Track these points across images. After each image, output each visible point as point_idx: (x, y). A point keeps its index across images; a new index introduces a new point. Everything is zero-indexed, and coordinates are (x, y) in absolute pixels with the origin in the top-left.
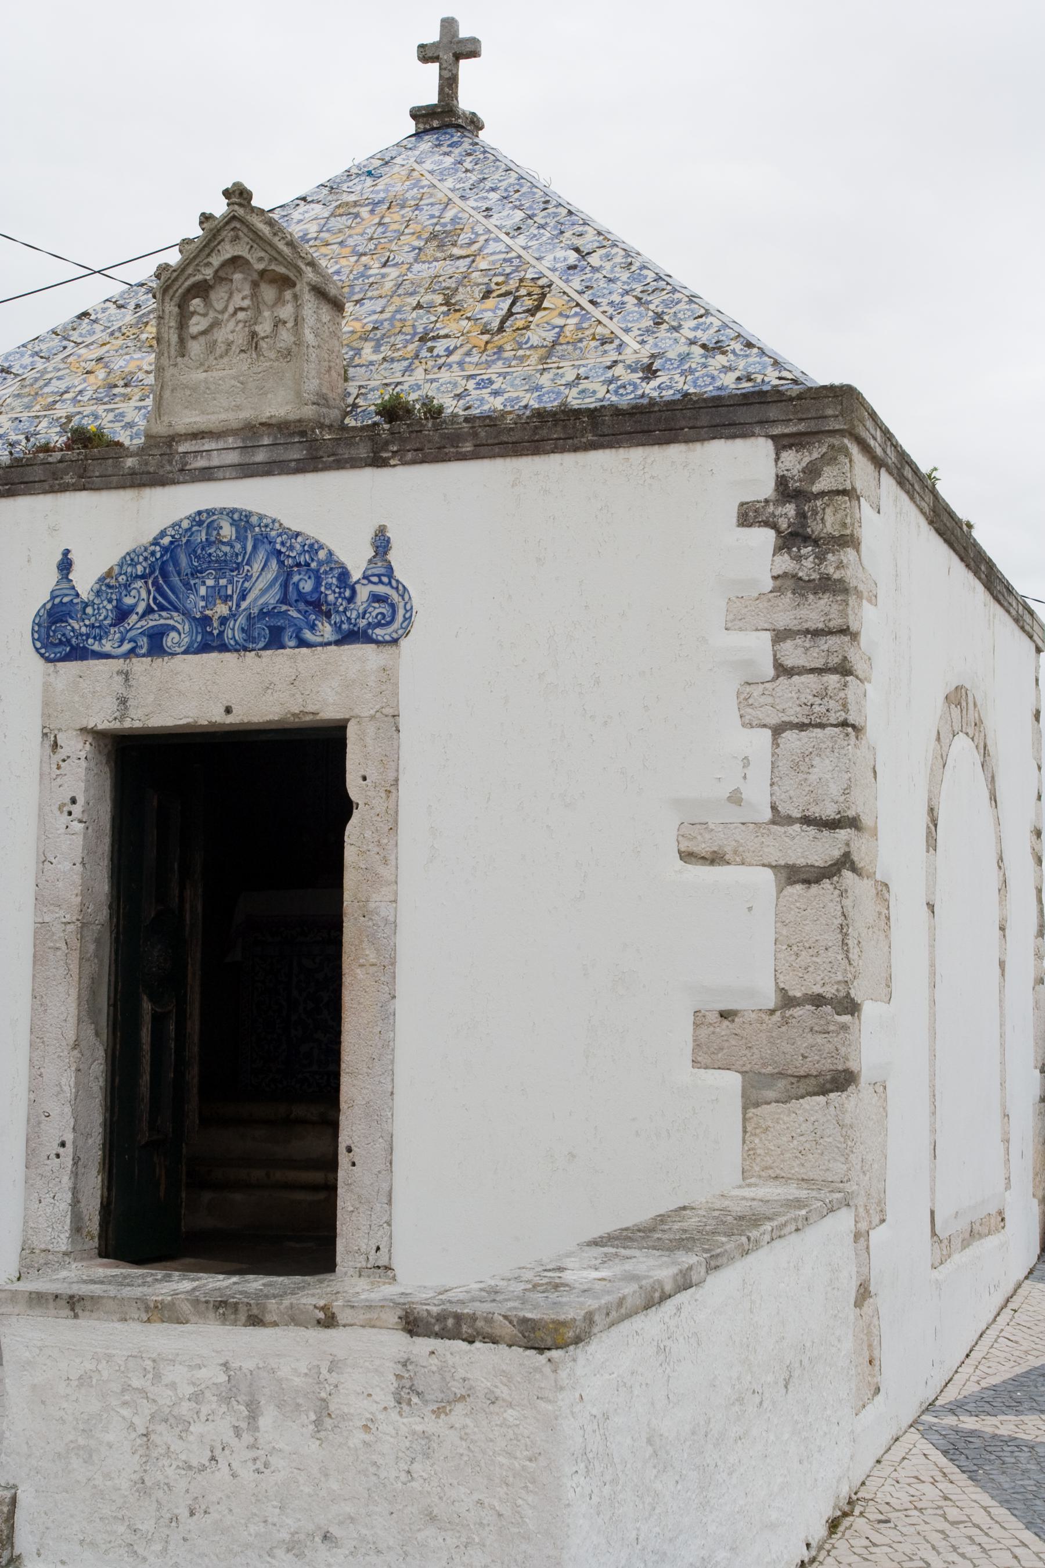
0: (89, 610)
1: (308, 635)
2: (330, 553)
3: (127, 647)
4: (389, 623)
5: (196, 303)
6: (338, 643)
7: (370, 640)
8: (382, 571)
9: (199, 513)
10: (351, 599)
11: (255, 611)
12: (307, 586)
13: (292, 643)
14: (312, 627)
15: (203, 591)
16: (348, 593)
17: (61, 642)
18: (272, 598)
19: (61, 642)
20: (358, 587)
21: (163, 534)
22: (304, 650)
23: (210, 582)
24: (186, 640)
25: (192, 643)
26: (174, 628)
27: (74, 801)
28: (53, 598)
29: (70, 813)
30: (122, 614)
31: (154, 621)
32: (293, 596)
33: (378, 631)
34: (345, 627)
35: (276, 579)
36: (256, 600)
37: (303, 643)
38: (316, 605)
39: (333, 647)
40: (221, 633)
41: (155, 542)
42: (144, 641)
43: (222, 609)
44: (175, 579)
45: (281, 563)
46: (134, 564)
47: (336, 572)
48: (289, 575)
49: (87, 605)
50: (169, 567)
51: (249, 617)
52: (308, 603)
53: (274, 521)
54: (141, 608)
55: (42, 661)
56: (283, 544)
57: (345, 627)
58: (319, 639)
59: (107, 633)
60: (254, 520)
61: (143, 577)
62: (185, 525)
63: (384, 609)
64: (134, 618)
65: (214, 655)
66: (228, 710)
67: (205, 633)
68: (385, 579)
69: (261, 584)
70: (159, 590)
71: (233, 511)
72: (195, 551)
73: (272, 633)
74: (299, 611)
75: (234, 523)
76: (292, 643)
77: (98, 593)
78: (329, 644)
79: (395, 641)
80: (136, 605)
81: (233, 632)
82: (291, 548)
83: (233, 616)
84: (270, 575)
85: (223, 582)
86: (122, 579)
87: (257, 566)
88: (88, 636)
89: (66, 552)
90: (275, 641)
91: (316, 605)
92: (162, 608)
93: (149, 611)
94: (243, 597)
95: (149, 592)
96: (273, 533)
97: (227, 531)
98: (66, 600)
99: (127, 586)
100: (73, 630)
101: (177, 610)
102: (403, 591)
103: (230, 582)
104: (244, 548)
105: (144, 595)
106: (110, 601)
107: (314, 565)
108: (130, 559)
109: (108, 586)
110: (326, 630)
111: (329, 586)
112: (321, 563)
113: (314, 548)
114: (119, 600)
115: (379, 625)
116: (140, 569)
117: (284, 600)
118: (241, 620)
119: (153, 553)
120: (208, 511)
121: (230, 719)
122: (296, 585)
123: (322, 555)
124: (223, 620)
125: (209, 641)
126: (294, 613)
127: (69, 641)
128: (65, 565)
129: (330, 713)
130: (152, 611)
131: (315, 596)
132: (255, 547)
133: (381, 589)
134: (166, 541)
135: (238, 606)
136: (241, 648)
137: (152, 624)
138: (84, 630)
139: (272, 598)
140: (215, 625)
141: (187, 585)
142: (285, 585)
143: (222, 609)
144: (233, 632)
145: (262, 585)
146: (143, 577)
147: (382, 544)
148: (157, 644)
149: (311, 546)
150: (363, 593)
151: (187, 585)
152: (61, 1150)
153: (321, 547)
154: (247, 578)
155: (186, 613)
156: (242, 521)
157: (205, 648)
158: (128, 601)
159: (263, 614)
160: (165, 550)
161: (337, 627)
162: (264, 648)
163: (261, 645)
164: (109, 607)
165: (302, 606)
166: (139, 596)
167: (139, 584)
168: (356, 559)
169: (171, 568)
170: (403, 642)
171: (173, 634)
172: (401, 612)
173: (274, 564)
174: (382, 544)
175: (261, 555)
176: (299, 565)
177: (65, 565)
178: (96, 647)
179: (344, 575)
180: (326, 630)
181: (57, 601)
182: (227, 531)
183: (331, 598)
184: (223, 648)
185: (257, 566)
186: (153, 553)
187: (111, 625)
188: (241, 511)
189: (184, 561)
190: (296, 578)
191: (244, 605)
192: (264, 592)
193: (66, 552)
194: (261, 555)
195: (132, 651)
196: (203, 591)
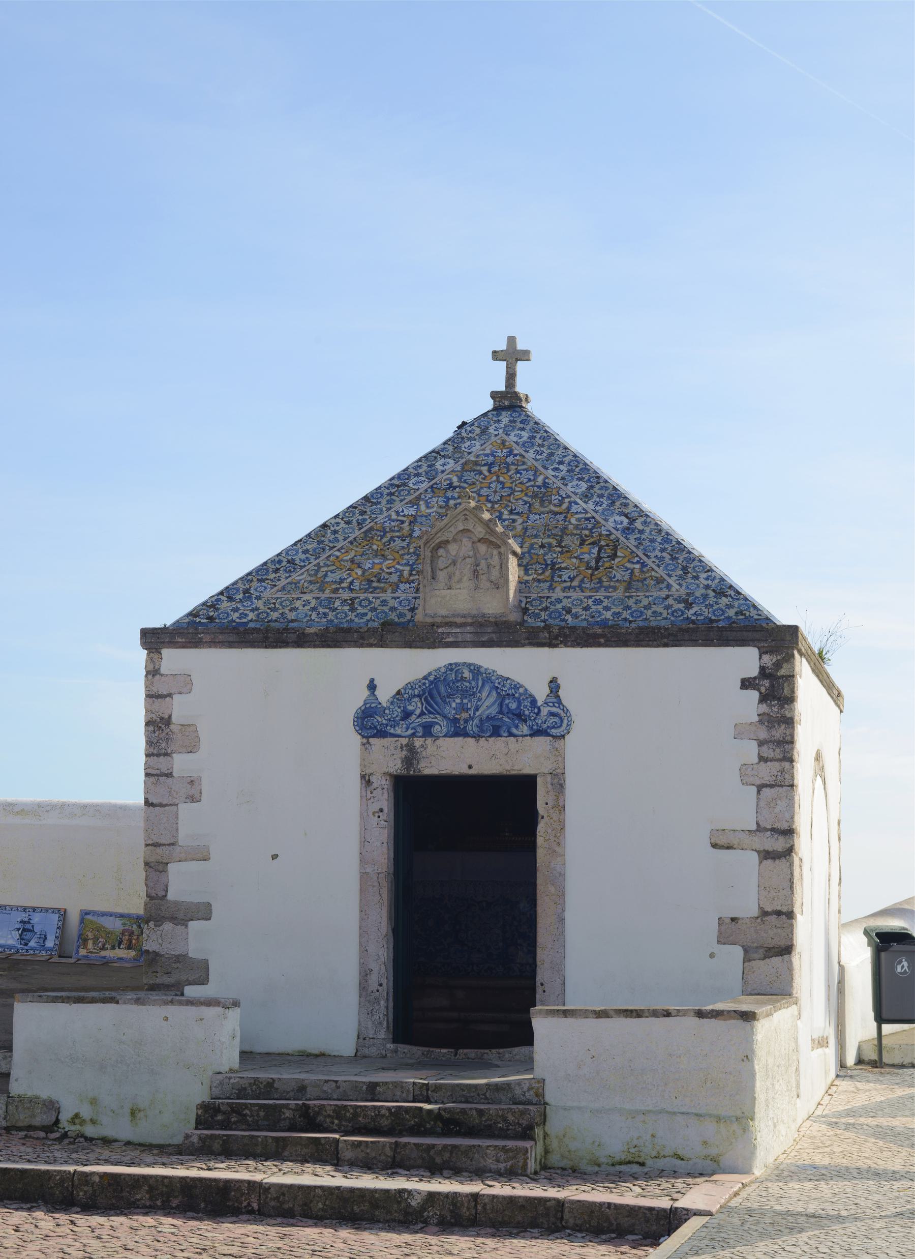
0: (387, 712)
1: (514, 731)
2: (526, 690)
3: (410, 732)
4: (559, 727)
5: (441, 552)
6: (531, 735)
7: (548, 735)
8: (555, 700)
9: (451, 664)
10: (538, 714)
11: (485, 716)
12: (513, 706)
13: (506, 734)
14: (517, 727)
15: (454, 705)
16: (536, 711)
17: (371, 727)
18: (494, 710)
19: (371, 727)
20: (542, 708)
21: (430, 674)
22: (512, 738)
23: (458, 701)
24: (445, 730)
25: (448, 731)
26: (437, 723)
27: (381, 810)
28: (365, 704)
29: (379, 817)
30: (407, 715)
31: (426, 719)
32: (505, 710)
33: (553, 730)
34: (535, 727)
35: (495, 701)
36: (485, 711)
37: (511, 735)
38: (519, 716)
39: (528, 738)
40: (465, 727)
41: (425, 678)
42: (420, 730)
43: (465, 715)
44: (438, 699)
45: (498, 693)
46: (413, 688)
47: (529, 700)
48: (503, 700)
49: (385, 709)
50: (433, 691)
51: (481, 720)
52: (513, 714)
53: (494, 671)
54: (418, 712)
55: (359, 737)
56: (499, 683)
57: (535, 727)
58: (520, 733)
59: (398, 724)
60: (482, 670)
61: (419, 696)
62: (443, 670)
63: (556, 720)
64: (414, 717)
65: (461, 738)
66: (470, 767)
67: (455, 727)
68: (556, 705)
69: (487, 703)
70: (428, 703)
71: (470, 665)
72: (449, 684)
73: (494, 728)
74: (509, 718)
75: (470, 671)
76: (506, 734)
77: (392, 703)
78: (526, 736)
79: (563, 737)
80: (414, 710)
81: (472, 727)
82: (504, 686)
83: (472, 719)
84: (491, 699)
85: (465, 701)
86: (406, 696)
87: (484, 694)
88: (387, 725)
89: (372, 681)
90: (496, 733)
91: (519, 716)
92: (430, 713)
93: (422, 714)
94: (477, 709)
95: (422, 704)
96: (493, 678)
97: (467, 674)
98: (373, 705)
99: (409, 700)
100: (378, 721)
101: (439, 714)
102: (566, 710)
103: (470, 701)
104: (477, 684)
105: (419, 705)
106: (399, 707)
107: (517, 695)
108: (410, 686)
109: (398, 699)
110: (525, 729)
111: (526, 707)
112: (521, 694)
113: (517, 686)
114: (405, 707)
115: (554, 727)
116: (416, 692)
117: (501, 712)
118: (476, 721)
119: (424, 684)
120: (455, 664)
121: (471, 772)
122: (507, 705)
123: (521, 690)
124: (466, 721)
125: (458, 731)
126: (507, 720)
127: (375, 727)
128: (372, 686)
129: (527, 771)
130: (425, 714)
131: (518, 711)
132: (483, 685)
133: (554, 710)
134: (432, 678)
135: (474, 714)
136: (477, 737)
137: (424, 720)
138: (384, 722)
139: (494, 710)
140: (462, 722)
141: (444, 701)
142: (501, 705)
143: (465, 715)
144: (472, 727)
145: (488, 704)
146: (419, 696)
147: (554, 686)
148: (427, 730)
149: (515, 685)
150: (545, 711)
151: (444, 701)
152: (380, 988)
153: (522, 686)
154: (479, 700)
155: (445, 717)
156: (476, 670)
157: (456, 734)
158: (410, 708)
159: (489, 718)
160: (431, 683)
161: (531, 728)
162: (490, 736)
163: (488, 734)
164: (399, 710)
165: (510, 715)
166: (416, 706)
167: (417, 699)
168: (541, 693)
169: (435, 692)
170: (567, 737)
171: (437, 727)
172: (566, 722)
173: (494, 693)
174: (554, 686)
175: (487, 688)
176: (508, 695)
177: (372, 686)
178: (392, 731)
179: (534, 702)
180: (525, 729)
181: (368, 706)
182: (467, 674)
183: (527, 712)
184: (466, 735)
185: (484, 694)
186: (424, 684)
187: (402, 720)
188: (474, 665)
189: (442, 689)
190: (507, 701)
191: (478, 714)
192: (488, 707)
193: (372, 681)
194: (487, 688)
195: (413, 735)
196: (454, 705)
